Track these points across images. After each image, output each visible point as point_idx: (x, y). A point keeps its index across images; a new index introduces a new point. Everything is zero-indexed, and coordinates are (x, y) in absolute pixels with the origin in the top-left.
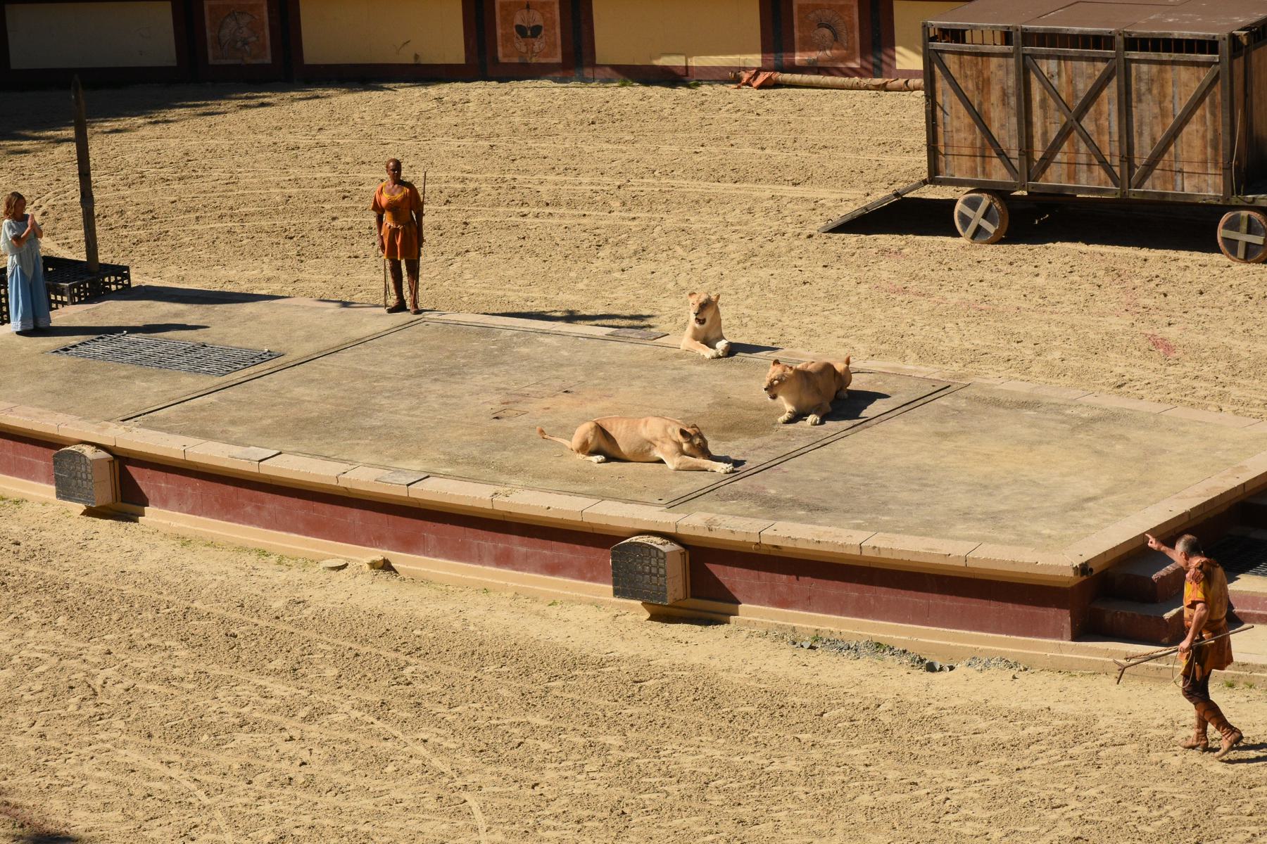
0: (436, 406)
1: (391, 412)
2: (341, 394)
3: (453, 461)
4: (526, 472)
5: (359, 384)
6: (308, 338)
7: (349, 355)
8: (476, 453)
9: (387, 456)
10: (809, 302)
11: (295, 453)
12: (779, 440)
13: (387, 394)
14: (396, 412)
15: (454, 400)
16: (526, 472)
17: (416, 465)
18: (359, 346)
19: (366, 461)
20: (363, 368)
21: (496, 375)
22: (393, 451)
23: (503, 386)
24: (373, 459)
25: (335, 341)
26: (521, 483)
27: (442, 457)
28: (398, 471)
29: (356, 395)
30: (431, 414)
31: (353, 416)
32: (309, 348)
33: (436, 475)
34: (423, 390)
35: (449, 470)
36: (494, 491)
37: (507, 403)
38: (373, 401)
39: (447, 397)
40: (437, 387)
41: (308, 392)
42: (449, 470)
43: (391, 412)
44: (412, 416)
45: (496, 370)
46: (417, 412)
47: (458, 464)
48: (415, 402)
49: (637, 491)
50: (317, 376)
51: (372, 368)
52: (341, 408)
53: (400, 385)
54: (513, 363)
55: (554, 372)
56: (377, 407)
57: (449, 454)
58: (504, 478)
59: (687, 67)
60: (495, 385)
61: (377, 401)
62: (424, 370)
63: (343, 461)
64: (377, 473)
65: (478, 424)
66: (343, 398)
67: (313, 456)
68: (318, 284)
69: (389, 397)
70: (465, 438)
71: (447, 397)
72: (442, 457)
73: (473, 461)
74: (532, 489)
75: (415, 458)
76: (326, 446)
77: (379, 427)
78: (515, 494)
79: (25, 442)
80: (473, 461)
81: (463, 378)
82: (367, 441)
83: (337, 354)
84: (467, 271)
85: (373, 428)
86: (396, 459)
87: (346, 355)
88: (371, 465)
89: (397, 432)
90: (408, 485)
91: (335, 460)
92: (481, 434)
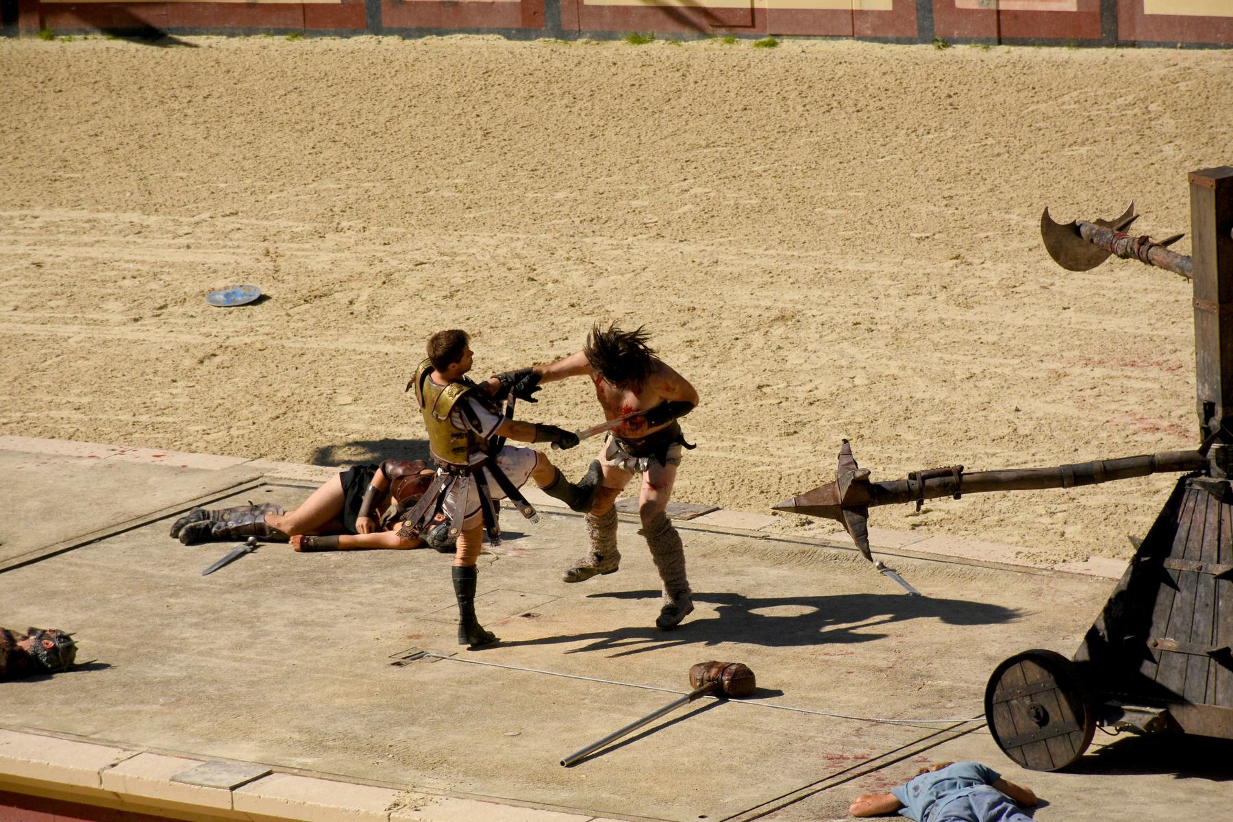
0: (284, 641)
1: (200, 653)
2: (108, 619)
3: (317, 744)
4: (453, 765)
5: (142, 601)
6: (47, 514)
7: (125, 545)
8: (359, 729)
9: (192, 735)
10: (980, 449)
11: (20, 729)
12: (924, 706)
13: (194, 620)
14: (210, 653)
15: (318, 632)
16: (453, 765)
17: (247, 753)
18: (142, 530)
19: (153, 743)
20: (150, 571)
21: (397, 585)
22: (205, 724)
23: (410, 605)
24: (167, 740)
25: (96, 520)
26: (443, 784)
27: (296, 736)
28: (215, 762)
29: (135, 621)
30: (276, 657)
31: (129, 661)
32: (49, 533)
33: (285, 770)
34: (261, 611)
35: (309, 761)
36: (393, 800)
37: (418, 637)
38: (167, 633)
39: (305, 624)
40: (290, 607)
41: (46, 614)
42: (309, 761)
43: (200, 653)
44: (241, 660)
45: (396, 575)
46: (250, 654)
47: (327, 749)
48: (245, 633)
49: (658, 802)
50: (62, 585)
51: (166, 571)
52: (109, 645)
53: (218, 604)
54: (430, 561)
55: (506, 580)
56: (174, 644)
57: (309, 732)
58: (410, 776)
59: (753, 10)
60: (397, 603)
61: (175, 632)
62: (265, 575)
63: (111, 744)
64: (172, 765)
65: (363, 676)
66: (111, 626)
67: (54, 733)
68: (65, 413)
69: (196, 625)
70: (338, 702)
71: (305, 624)
72: (296, 736)
73: (350, 744)
74: (463, 796)
75: (246, 735)
76: (79, 716)
77: (179, 681)
78: (431, 807)
79: (11, 804)
80: (350, 744)
81: (336, 590)
82: (156, 707)
83: (101, 545)
84: (344, 390)
85: (167, 683)
86: (211, 740)
87: (117, 545)
88: (162, 752)
89: (211, 690)
90: (233, 788)
91: (95, 742)
92: (370, 694)
